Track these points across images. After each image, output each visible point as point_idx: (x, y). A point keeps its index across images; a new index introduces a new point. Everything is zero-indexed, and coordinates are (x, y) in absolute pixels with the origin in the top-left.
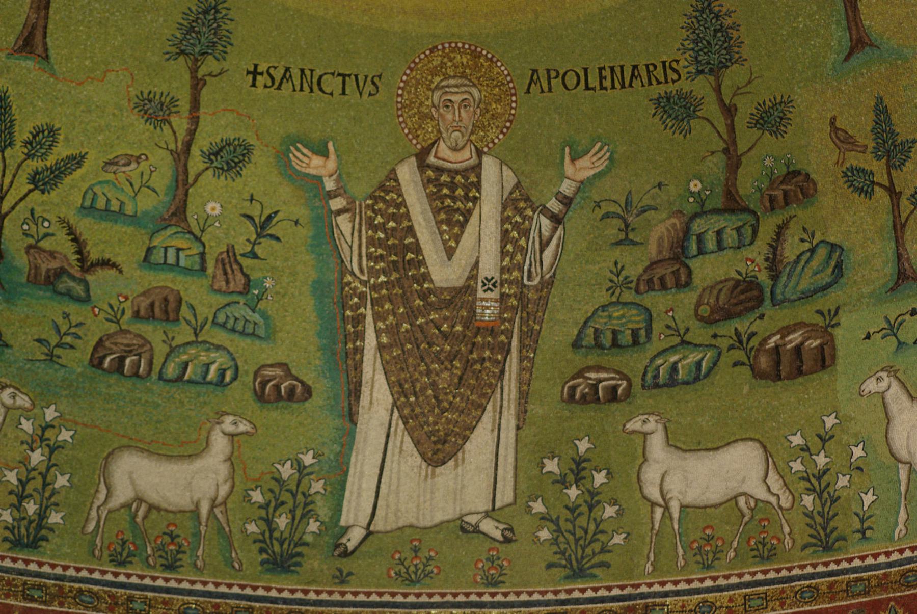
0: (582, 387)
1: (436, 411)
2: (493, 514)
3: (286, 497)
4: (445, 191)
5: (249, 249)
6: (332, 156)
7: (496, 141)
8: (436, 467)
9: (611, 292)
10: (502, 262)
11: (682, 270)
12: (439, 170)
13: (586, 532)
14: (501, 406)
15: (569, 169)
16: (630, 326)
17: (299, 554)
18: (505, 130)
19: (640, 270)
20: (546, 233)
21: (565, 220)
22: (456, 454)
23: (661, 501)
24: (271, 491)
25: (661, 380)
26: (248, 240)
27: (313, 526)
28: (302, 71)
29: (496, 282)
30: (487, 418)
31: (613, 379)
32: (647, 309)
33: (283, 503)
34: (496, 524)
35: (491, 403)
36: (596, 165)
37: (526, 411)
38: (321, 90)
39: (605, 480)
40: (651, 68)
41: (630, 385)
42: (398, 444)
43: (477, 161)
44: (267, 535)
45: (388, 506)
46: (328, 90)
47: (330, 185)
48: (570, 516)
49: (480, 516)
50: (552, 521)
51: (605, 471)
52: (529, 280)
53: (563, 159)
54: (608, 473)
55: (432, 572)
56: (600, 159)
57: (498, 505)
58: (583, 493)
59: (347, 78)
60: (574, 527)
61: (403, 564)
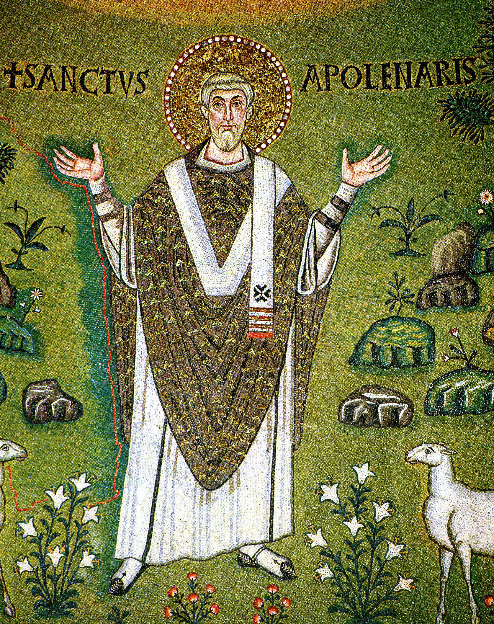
0: (361, 407)
1: (210, 428)
2: (272, 546)
3: (58, 527)
4: (216, 194)
5: (15, 259)
6: (98, 159)
7: (269, 141)
8: (211, 490)
9: (390, 305)
10: (274, 270)
11: (468, 287)
12: (210, 172)
13: (369, 572)
14: (276, 424)
15: (346, 173)
16: (411, 343)
17: (74, 593)
18: (279, 130)
19: (422, 282)
20: (321, 241)
21: (342, 226)
22: (230, 476)
23: (449, 545)
24: (44, 522)
25: (446, 406)
26: (14, 250)
27: (88, 560)
28: (64, 68)
29: (269, 290)
30: (261, 436)
31: (392, 401)
32: (429, 327)
33: (56, 535)
34: (275, 558)
35: (265, 420)
36: (376, 169)
37: (301, 431)
38: (85, 88)
39: (388, 515)
40: (441, 66)
41: (411, 409)
42: (172, 465)
43: (250, 162)
44: (40, 572)
45: (163, 535)
46: (92, 88)
47: (95, 188)
48: (352, 553)
49: (258, 547)
50: (333, 557)
51: (388, 504)
52: (302, 290)
53: (340, 162)
54: (391, 506)
55: (211, 612)
56: (380, 163)
57: (276, 535)
58: (365, 527)
59: (112, 76)
60: (357, 567)
61: (180, 602)
